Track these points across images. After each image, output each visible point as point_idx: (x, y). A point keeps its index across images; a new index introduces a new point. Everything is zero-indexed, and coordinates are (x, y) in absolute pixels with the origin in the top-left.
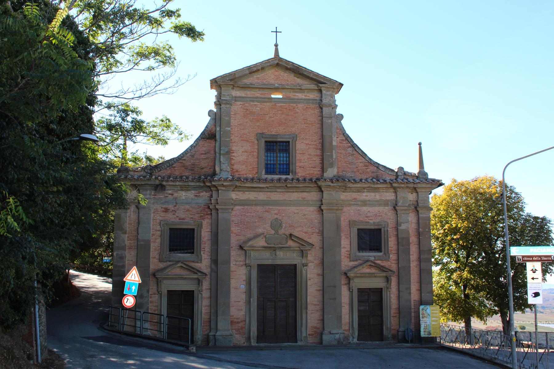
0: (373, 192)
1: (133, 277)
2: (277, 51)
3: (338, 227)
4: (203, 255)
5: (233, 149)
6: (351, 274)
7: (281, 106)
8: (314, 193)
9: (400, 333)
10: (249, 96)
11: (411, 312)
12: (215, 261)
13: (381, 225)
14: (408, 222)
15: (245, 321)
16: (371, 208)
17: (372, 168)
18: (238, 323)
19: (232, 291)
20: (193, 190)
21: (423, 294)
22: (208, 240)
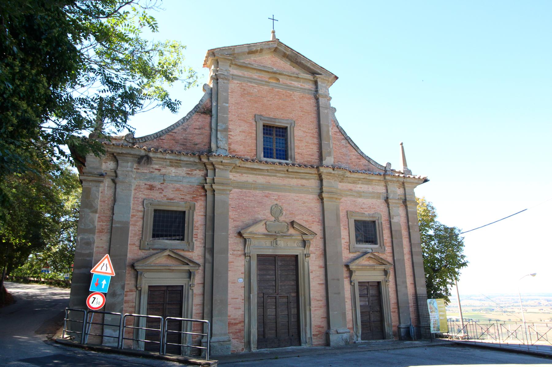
0: (366, 184)
1: (104, 268)
2: (274, 36)
3: (338, 216)
4: (195, 242)
5: (230, 127)
6: (352, 267)
7: (278, 92)
8: (313, 181)
9: (402, 330)
10: (246, 76)
11: (409, 307)
12: (210, 249)
13: (375, 217)
14: (398, 215)
15: (244, 322)
16: (366, 201)
17: (364, 162)
18: (236, 324)
19: (230, 285)
20: (184, 167)
21: (418, 288)
22: (201, 225)
